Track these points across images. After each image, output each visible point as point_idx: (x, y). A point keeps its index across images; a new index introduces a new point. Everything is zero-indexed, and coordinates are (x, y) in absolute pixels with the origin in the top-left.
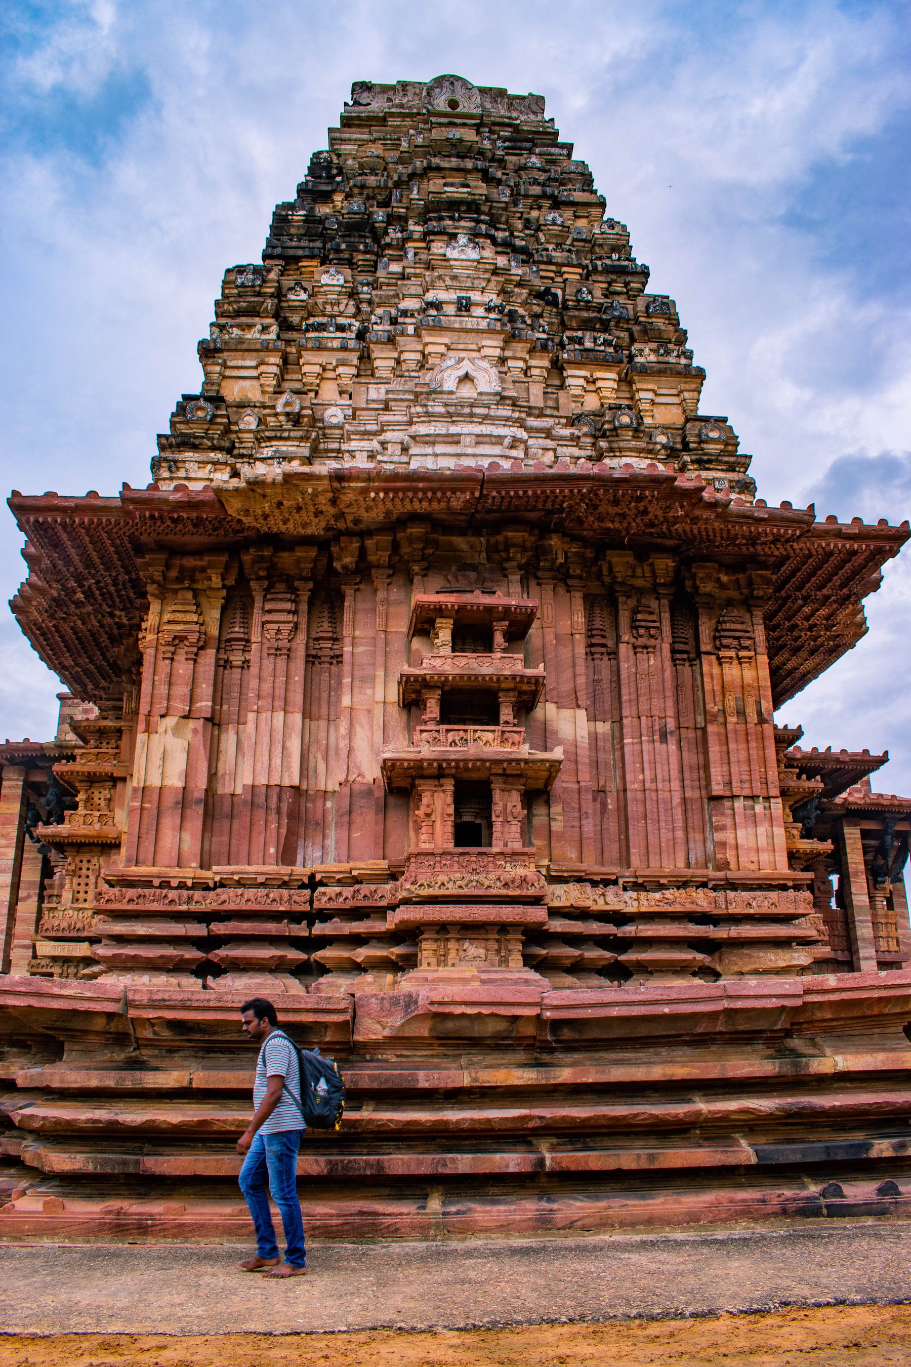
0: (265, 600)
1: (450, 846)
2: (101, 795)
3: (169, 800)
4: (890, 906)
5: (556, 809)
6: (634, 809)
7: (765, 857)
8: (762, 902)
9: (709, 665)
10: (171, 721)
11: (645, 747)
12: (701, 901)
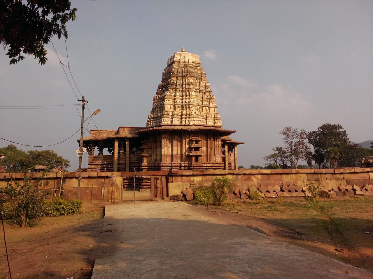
0: (175, 136)
1: (195, 162)
2: (147, 150)
3: (165, 156)
4: (231, 155)
5: (202, 157)
6: (208, 156)
7: (220, 161)
8: (219, 165)
9: (216, 142)
10: (165, 148)
11: (210, 151)
12: (214, 165)
